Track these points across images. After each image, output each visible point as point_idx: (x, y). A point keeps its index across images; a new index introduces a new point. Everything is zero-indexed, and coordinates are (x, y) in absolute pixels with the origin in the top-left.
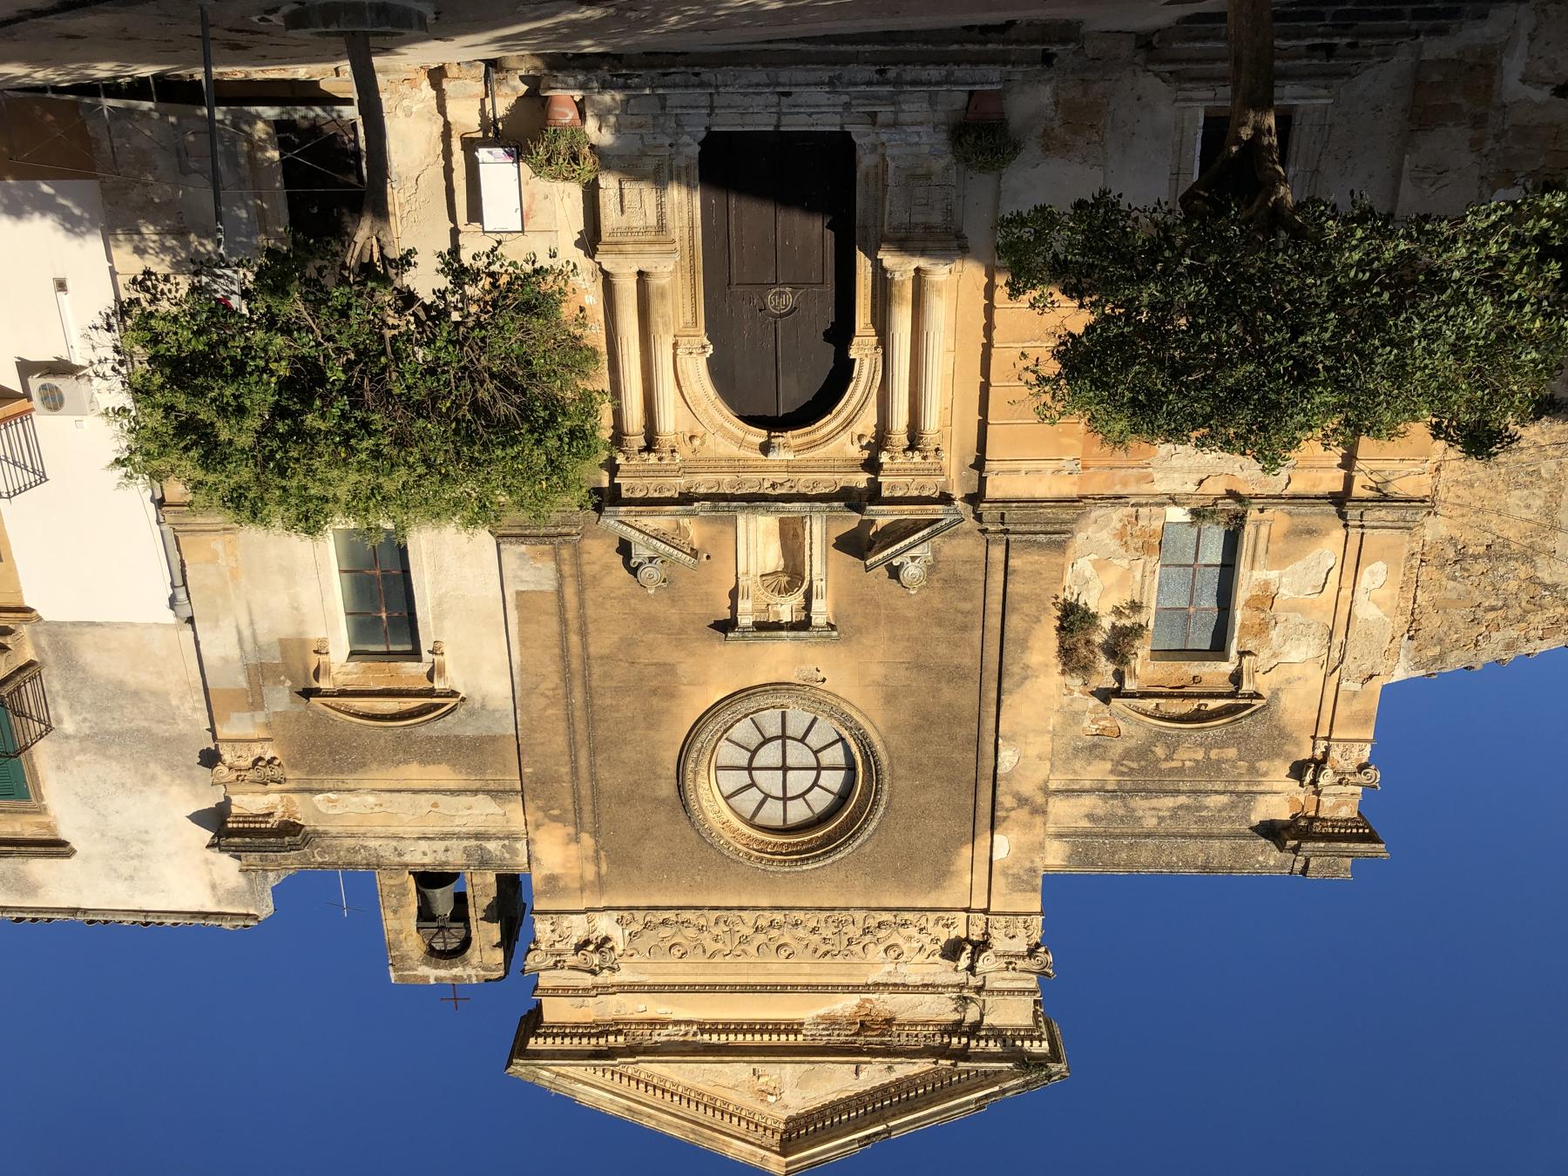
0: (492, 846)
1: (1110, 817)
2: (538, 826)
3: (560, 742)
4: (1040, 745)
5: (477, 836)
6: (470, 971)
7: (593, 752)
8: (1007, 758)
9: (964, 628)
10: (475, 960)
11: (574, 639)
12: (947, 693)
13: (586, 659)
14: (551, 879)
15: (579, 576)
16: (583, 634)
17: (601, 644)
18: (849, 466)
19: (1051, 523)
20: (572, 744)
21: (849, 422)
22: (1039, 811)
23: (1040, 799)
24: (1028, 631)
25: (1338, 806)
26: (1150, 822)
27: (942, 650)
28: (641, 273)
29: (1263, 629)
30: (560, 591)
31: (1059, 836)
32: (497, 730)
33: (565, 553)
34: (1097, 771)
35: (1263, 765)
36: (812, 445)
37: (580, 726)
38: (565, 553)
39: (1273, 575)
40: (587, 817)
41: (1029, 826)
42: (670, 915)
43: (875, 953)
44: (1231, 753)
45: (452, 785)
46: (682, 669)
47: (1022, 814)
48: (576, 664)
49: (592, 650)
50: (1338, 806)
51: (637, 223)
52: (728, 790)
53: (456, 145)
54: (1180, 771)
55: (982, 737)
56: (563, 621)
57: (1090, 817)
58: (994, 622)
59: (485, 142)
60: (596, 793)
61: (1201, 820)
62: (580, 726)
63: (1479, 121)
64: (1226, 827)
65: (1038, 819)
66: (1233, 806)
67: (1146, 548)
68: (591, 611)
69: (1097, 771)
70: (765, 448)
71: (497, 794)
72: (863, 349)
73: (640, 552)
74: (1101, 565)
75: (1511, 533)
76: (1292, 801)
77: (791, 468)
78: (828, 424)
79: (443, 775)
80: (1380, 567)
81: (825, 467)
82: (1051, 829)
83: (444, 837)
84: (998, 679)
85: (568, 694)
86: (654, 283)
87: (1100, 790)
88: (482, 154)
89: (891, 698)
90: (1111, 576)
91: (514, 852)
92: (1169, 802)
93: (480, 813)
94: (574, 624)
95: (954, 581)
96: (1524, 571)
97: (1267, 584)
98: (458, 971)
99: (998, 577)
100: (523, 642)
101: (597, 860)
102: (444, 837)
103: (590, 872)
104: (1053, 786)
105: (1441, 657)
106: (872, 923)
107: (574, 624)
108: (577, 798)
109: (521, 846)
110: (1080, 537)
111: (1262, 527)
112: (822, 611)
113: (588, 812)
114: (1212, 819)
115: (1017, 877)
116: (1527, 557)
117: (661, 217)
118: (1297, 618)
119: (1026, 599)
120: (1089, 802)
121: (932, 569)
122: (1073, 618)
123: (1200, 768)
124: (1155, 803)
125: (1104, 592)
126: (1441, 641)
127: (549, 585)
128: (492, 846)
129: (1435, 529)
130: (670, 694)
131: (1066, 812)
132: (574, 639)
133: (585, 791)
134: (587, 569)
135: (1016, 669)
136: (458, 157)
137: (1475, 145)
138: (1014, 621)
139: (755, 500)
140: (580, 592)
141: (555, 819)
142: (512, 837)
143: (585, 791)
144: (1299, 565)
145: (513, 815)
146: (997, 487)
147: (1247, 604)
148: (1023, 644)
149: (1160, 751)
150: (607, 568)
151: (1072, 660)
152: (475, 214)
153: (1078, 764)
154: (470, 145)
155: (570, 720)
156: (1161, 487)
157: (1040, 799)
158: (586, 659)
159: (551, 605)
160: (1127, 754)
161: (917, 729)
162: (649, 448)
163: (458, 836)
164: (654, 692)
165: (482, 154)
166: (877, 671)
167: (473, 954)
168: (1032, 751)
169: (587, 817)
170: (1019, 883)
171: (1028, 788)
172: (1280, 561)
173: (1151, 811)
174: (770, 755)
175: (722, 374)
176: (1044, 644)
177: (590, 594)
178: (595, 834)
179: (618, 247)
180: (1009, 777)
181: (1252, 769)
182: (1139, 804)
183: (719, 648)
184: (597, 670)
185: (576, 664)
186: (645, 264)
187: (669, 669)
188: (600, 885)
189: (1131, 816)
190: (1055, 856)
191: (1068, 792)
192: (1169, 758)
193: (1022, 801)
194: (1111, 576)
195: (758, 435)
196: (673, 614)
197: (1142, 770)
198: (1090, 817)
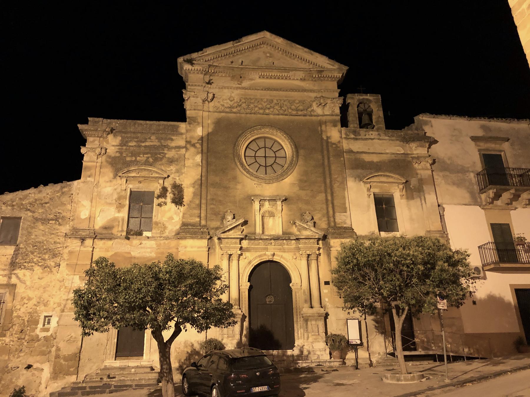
0: (353, 136)
1: (166, 139)
2: (339, 142)
3: (333, 167)
4: (188, 163)
5: (357, 139)
6: (358, 97)
7: (323, 164)
8: (198, 158)
10: (356, 100)
11: (329, 198)
12: (217, 179)
13: (326, 192)
14: (335, 126)
15: (328, 217)
16: (327, 200)
17: (321, 197)
18: (248, 250)
19: (187, 230)
20: (329, 167)
21: (250, 263)
23: (188, 146)
24: (193, 198)
26: (153, 138)
28: (312, 307)
29: (120, 198)
30: (334, 213)
31: (182, 134)
33: (332, 224)
34: (170, 154)
35: (118, 155)
36: (260, 256)
38: (332, 224)
39: (117, 215)
40: (325, 144)
41: (192, 137)
42: (300, 113)
43: (237, 99)
44: (128, 159)
45: (364, 155)
46: (298, 188)
47: (194, 141)
49: (324, 195)
50: (94, 141)
51: (313, 322)
52: (282, 151)
53: (365, 344)
54: (144, 154)
55: (208, 165)
56: (333, 204)
57: (172, 140)
58: (203, 201)
60: (322, 152)
61: (137, 138)
63: (57, 357)
64: (129, 135)
65: (188, 139)
66: (127, 142)
67: (157, 223)
68: (325, 206)
69: (170, 154)
70: (274, 254)
71: (350, 151)
72: (246, 285)
73: (311, 224)
74: (171, 218)
75: (42, 227)
76: (108, 142)
77: (267, 249)
78: (256, 262)
79: (367, 158)
81: (256, 250)
82: (184, 136)
83: (366, 139)
84: (202, 184)
85: (331, 182)
86: (308, 305)
87: (170, 148)
88: (359, 342)
89: (235, 178)
91: (346, 134)
92: (147, 144)
93: (357, 146)
95: (216, 214)
96: (36, 215)
97: (119, 211)
98: (361, 97)
99: (203, 215)
100: (344, 197)
101: (321, 131)
102: (366, 139)
103: (323, 127)
104: (184, 150)
105: (62, 188)
106: (239, 109)
110: (178, 227)
111: (120, 230)
112: (256, 205)
114: (134, 138)
115: (195, 122)
116: (37, 220)
117: (307, 324)
118: (108, 201)
119: (194, 208)
120: (173, 144)
121: (223, 218)
122: (178, 201)
123: (138, 154)
124: (152, 144)
125: (170, 210)
126: (63, 193)
127: (337, 214)
129: (65, 229)
130: (301, 181)
132: (329, 198)
133: (325, 152)
134: (325, 219)
135: (197, 187)
136: (365, 341)
137: (58, 349)
138: (197, 202)
139: (276, 238)
140: (328, 212)
141: (334, 144)
144: (109, 218)
145: (346, 145)
146: (204, 243)
147: (124, 206)
148: (195, 194)
149: (151, 160)
150: (320, 219)
151: (178, 189)
152: (360, 323)
153: (176, 156)
154: (361, 344)
155: (330, 174)
156: (152, 243)
157: (188, 146)
158: (326, 192)
159: (336, 208)
160: (161, 159)
162: (309, 255)
164: (306, 182)
165: (359, 342)
166: (239, 187)
168: (191, 161)
169: (325, 144)
170: (194, 120)
171: (192, 150)
172: (115, 219)
173: (153, 141)
174: (270, 161)
175: (287, 278)
176: (188, 194)
177: (325, 212)
178: (322, 139)
179: (320, 315)
181: (121, 153)
182: (157, 143)
183: (287, 195)
184: (323, 188)
185: (329, 191)
186: (311, 311)
187: (302, 188)
188: (320, 123)
189: (159, 139)
190: (183, 126)
191: (179, 147)
192: (148, 158)
193: (194, 145)
194: (168, 215)
195: (276, 259)
197: (156, 154)
198: (172, 140)
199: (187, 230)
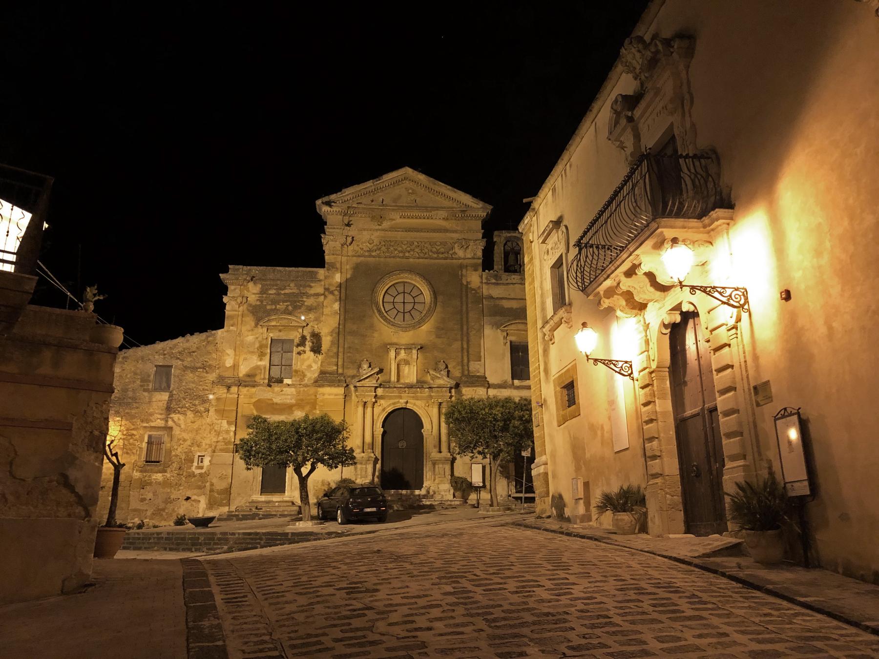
0: (494, 281)
1: (305, 286)
2: (479, 288)
3: (471, 315)
4: (326, 311)
5: (497, 284)
6: (504, 235)
7: (461, 310)
8: (336, 306)
9: (350, 348)
10: (503, 239)
11: (465, 346)
12: (355, 327)
13: (462, 340)
14: (476, 270)
15: (463, 366)
16: (462, 348)
17: (457, 345)
18: (382, 397)
19: (325, 378)
20: (467, 313)
21: (384, 410)
22: (326, 289)
23: (327, 293)
24: (331, 347)
25: (235, 289)
26: (292, 285)
27: (356, 341)
28: (440, 452)
29: (261, 346)
30: (468, 361)
31: (320, 281)
32: (489, 318)
33: (466, 373)
34: (309, 302)
35: (258, 303)
36: (394, 404)
37: (465, 319)
38: (466, 373)
39: (260, 363)
40: (464, 290)
41: (330, 285)
42: (441, 256)
43: (376, 242)
44: (268, 307)
45: (504, 301)
46: (434, 336)
47: (332, 288)
48: (465, 338)
49: (460, 343)
50: (235, 289)
51: (441, 466)
52: (421, 296)
53: (488, 487)
54: (284, 302)
55: (346, 314)
56: (468, 352)
57: (311, 287)
58: (341, 350)
59: (480, 487)
60: (461, 298)
61: (277, 285)
62: (465, 319)
63: (211, 491)
64: (268, 283)
65: (327, 286)
66: (267, 290)
67: (296, 371)
68: (460, 354)
69: (309, 302)
70: (407, 402)
71: (491, 297)
72: (379, 430)
73: (444, 373)
74: (310, 366)
75: (191, 375)
76: (248, 291)
77: (401, 397)
78: (390, 409)
79: (506, 304)
80: (228, 365)
81: (390, 398)
82: (323, 283)
83: (508, 284)
84: (339, 333)
85: (468, 329)
86: (437, 449)
87: (308, 296)
88: (481, 484)
89: (372, 327)
90: (307, 363)
91: (487, 279)
92: (287, 291)
93: (496, 292)
94: (465, 351)
95: (353, 362)
96: (185, 363)
97: (261, 360)
98: (509, 235)
99: (340, 363)
100: (480, 345)
101: (462, 275)
102: (508, 284)
103: (464, 271)
104: (322, 297)
105: (208, 337)
106: (378, 252)
107: (465, 351)
108: (467, 295)
109: (484, 281)
110: (316, 375)
111: (262, 378)
112: (392, 354)
113: (465, 290)
114: (273, 285)
115: (333, 267)
116: (186, 367)
117: (434, 468)
118: (251, 349)
119: (332, 357)
120: (312, 291)
121: (360, 366)
122: (316, 349)
123: (278, 302)
124: (291, 291)
125: (309, 358)
126: (208, 342)
127: (471, 363)
128: (494, 281)
129: (212, 377)
130: (438, 328)
131: (318, 289)
132: (465, 346)
133: (464, 298)
134: (460, 367)
135: (334, 335)
136: (488, 484)
137: (212, 485)
138: (335, 350)
139: (410, 386)
140: (462, 361)
141: (474, 290)
142: (487, 283)
143: (464, 298)
144: (252, 366)
145: (486, 291)
146: (341, 390)
147: (266, 354)
148: (332, 342)
149: (290, 308)
150: (454, 367)
151: (316, 337)
152: (484, 468)
153: (315, 304)
154: (484, 486)
155: (467, 322)
156: (293, 390)
157: (327, 293)
158: (462, 340)
159: (471, 357)
160: (300, 307)
161: (364, 316)
162: (440, 404)
163: (503, 284)
164: (443, 329)
165: (481, 484)
166: (376, 335)
167: (503, 241)
168: (329, 309)
169: (464, 290)
170: (333, 266)
171: (331, 297)
172: (258, 367)
173: (292, 289)
174: (409, 307)
176: (326, 342)
177: (460, 360)
178: (462, 284)
179: (446, 460)
180: (336, 301)
181: (262, 301)
182: (296, 291)
183: (422, 342)
184: (459, 337)
185: (465, 338)
186: (439, 455)
187: (438, 336)
188: (461, 267)
189: (298, 286)
190: (321, 272)
191: (318, 295)
192: (287, 306)
193: (332, 293)
194: (307, 363)
195: (409, 406)
196: (436, 353)
197: (295, 302)
198: (311, 287)
199: (325, 378)
